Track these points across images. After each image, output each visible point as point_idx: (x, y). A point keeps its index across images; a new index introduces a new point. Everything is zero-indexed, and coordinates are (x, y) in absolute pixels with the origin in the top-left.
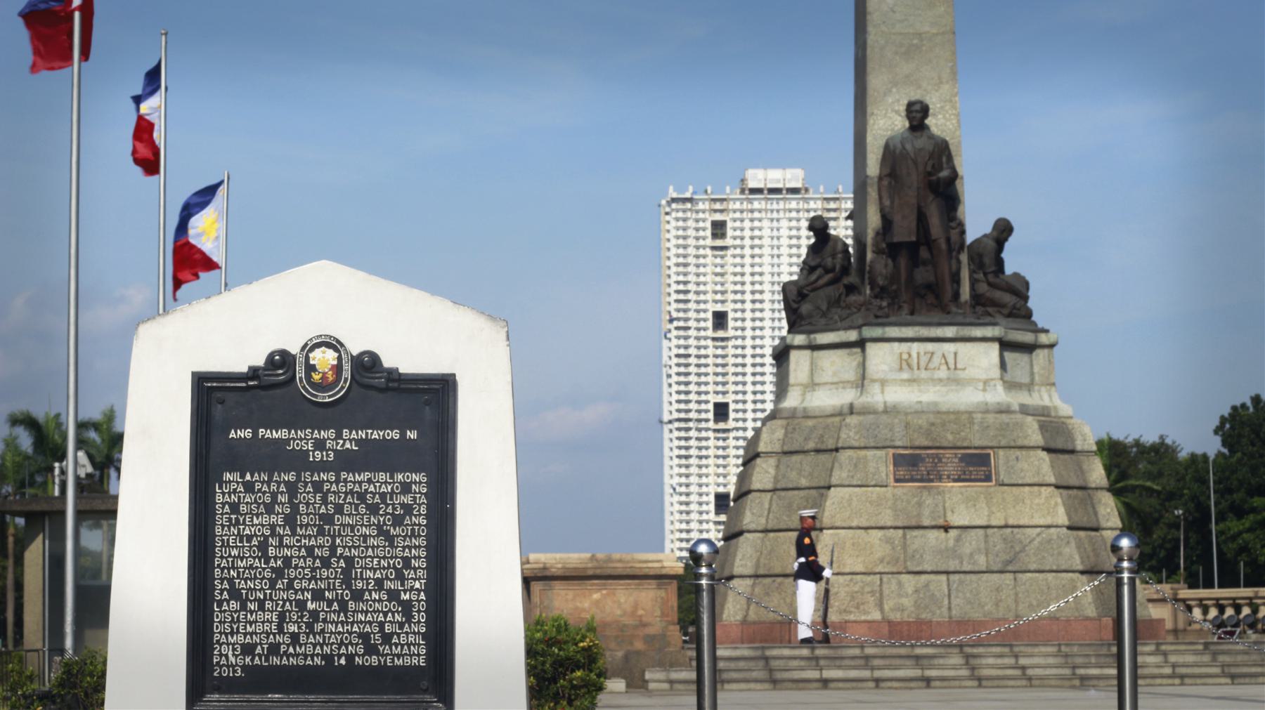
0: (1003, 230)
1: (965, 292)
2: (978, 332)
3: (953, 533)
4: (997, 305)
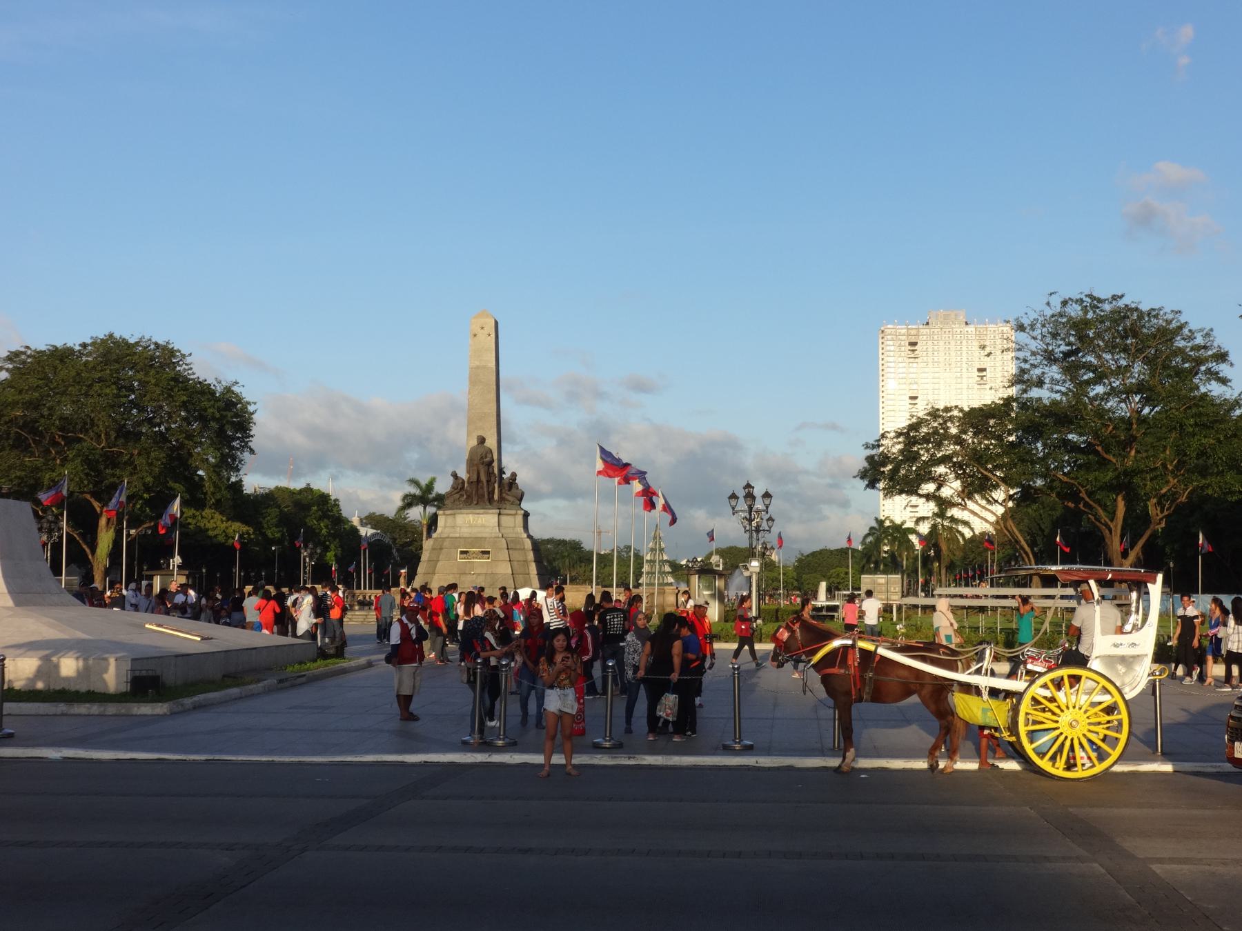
0: (514, 475)
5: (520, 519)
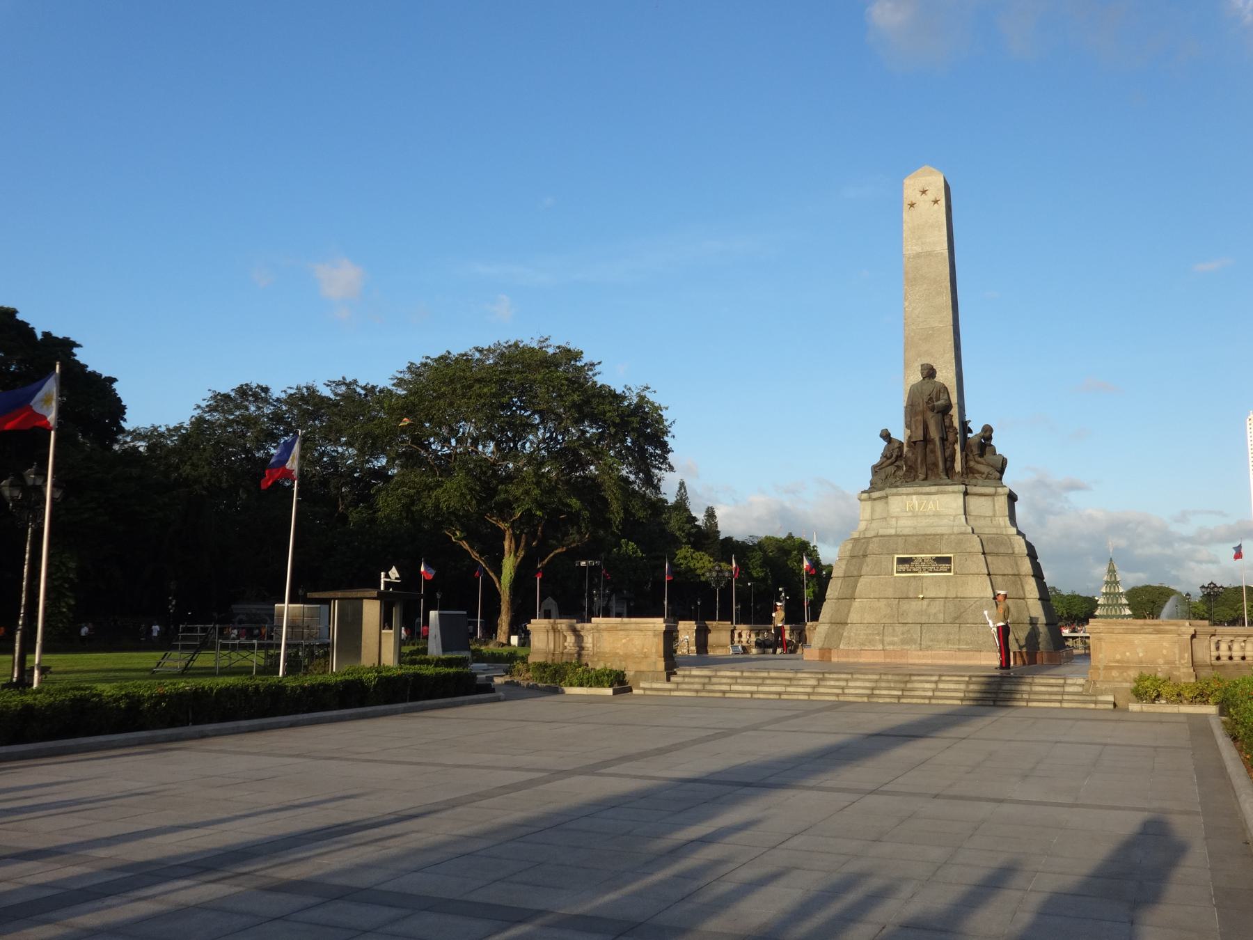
0: (988, 431)
2: (950, 488)
3: (925, 602)
5: (1002, 502)
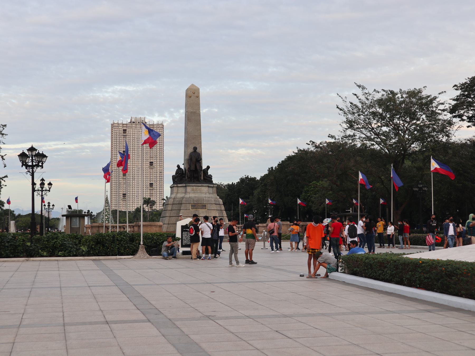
0: (208, 167)
1: (202, 178)
4: (207, 180)
